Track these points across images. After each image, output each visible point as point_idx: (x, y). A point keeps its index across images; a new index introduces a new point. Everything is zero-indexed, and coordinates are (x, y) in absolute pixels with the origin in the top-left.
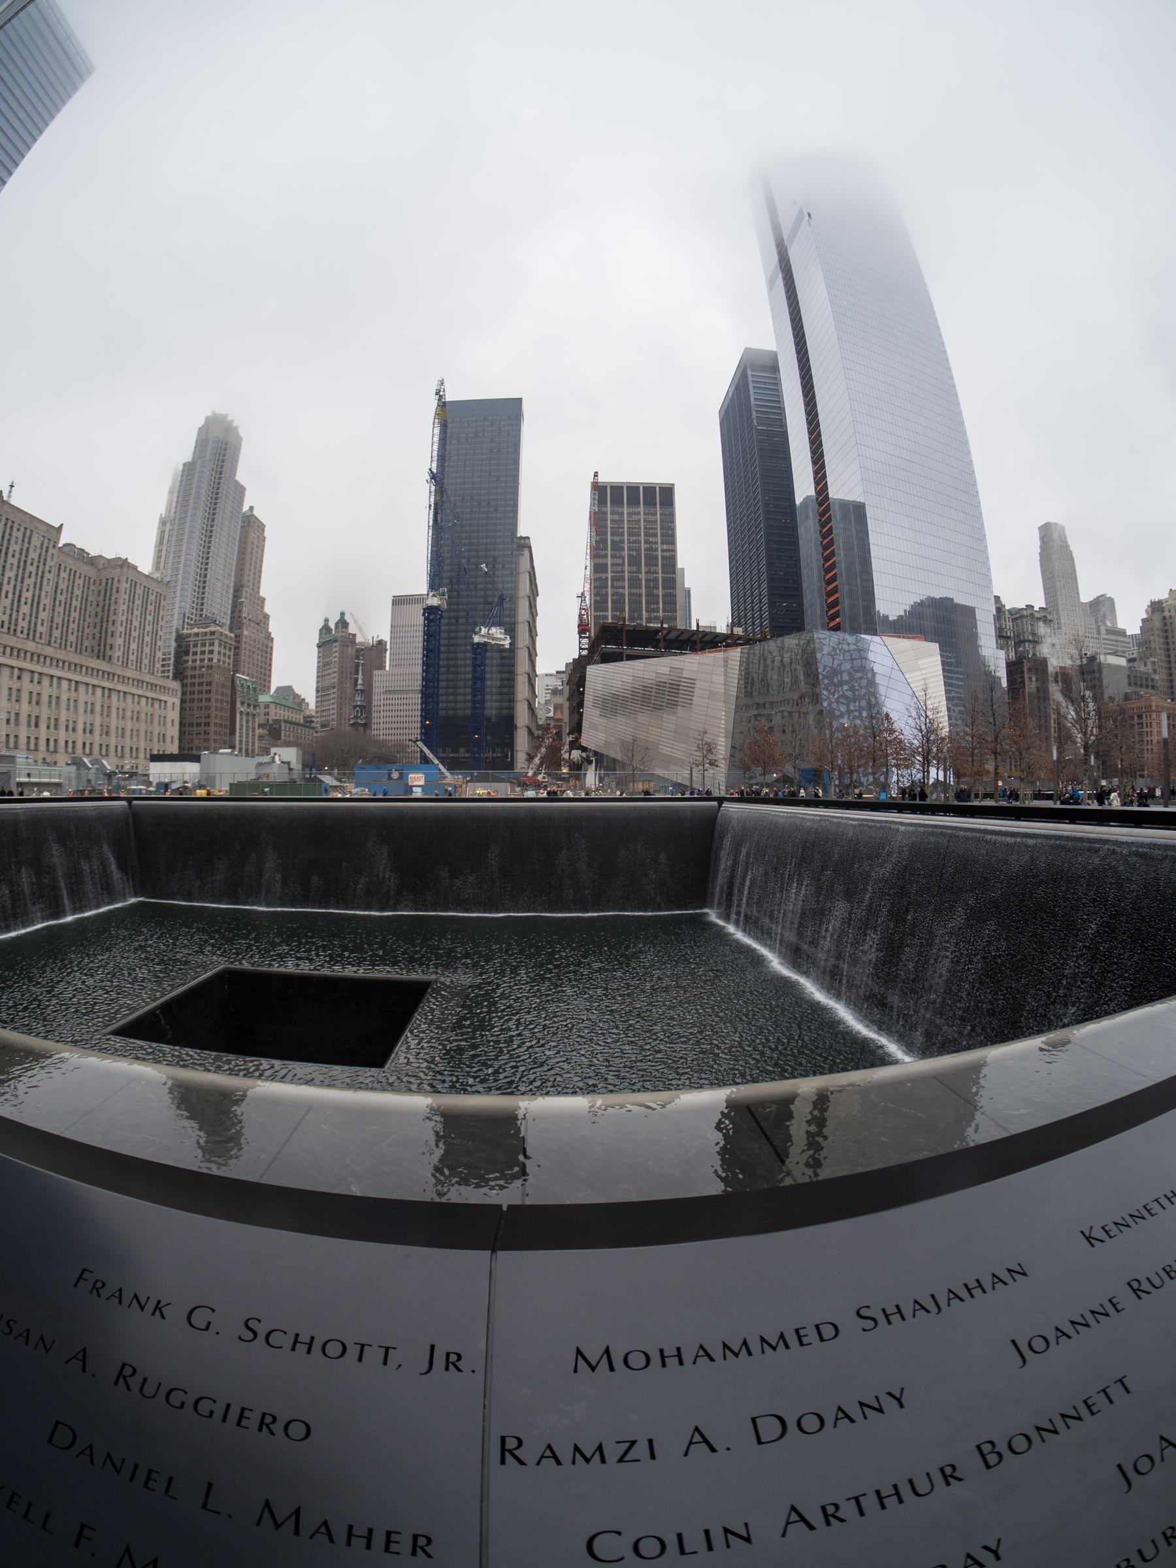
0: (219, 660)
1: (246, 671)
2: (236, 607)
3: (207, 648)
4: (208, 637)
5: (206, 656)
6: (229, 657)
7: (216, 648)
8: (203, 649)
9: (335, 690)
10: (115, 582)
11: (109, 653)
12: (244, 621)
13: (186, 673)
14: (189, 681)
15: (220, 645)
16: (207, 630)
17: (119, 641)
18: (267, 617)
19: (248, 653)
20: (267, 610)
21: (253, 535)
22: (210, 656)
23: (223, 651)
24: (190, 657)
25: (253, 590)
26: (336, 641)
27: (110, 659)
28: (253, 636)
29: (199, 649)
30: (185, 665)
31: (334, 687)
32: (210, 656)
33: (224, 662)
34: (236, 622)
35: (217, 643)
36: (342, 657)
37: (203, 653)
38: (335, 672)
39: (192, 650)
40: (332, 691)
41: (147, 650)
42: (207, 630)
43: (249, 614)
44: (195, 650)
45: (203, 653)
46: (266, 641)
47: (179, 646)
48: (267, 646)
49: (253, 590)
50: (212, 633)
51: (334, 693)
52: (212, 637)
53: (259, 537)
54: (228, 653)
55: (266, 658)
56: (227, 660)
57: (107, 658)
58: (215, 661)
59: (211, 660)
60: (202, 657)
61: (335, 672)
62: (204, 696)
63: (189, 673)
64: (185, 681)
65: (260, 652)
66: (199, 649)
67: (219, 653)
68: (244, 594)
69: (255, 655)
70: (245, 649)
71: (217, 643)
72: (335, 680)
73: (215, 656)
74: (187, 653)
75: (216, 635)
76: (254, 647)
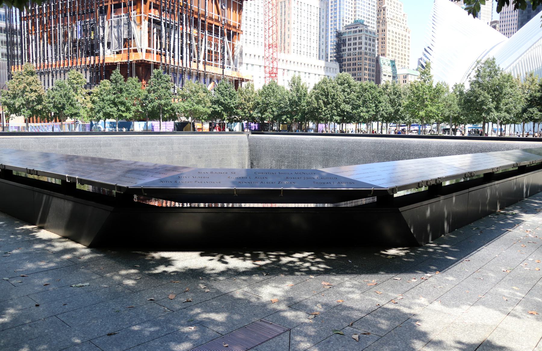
0: (366, 49)
3: (357, 41)
4: (358, 33)
5: (357, 46)
6: (374, 46)
7: (363, 40)
8: (355, 41)
10: (287, 3)
11: (287, 47)
12: (387, 20)
13: (344, 58)
14: (346, 62)
16: (357, 29)
17: (294, 39)
19: (391, 41)
22: (360, 46)
23: (368, 42)
24: (347, 47)
27: (288, 52)
29: (352, 42)
30: (343, 53)
32: (360, 46)
33: (370, 50)
35: (363, 38)
37: (355, 44)
39: (347, 42)
42: (357, 29)
44: (350, 42)
45: (355, 44)
47: (340, 40)
48: (405, 36)
50: (360, 31)
52: (360, 33)
54: (372, 43)
56: (372, 48)
57: (286, 51)
58: (363, 49)
59: (360, 48)
60: (355, 47)
62: (357, 72)
63: (346, 57)
64: (344, 63)
65: (400, 40)
66: (352, 42)
67: (366, 44)
69: (397, 43)
70: (389, 39)
71: (363, 38)
73: (363, 46)
74: (345, 45)
75: (364, 32)
76: (396, 37)
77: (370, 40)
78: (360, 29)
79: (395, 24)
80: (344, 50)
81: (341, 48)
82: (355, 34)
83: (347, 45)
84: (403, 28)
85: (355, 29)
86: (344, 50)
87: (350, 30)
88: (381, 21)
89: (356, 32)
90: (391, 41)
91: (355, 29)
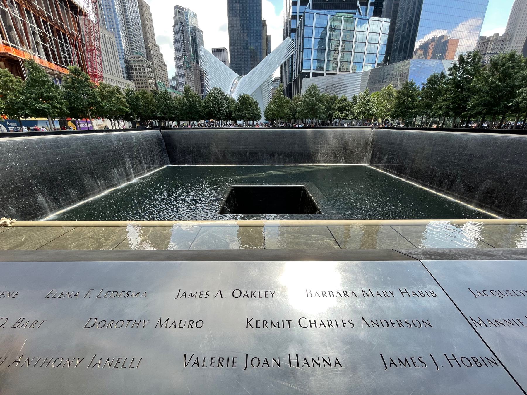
0: (148, 73)
1: (158, 79)
2: (147, 49)
4: (140, 62)
9: (194, 88)
15: (147, 67)
18: (161, 54)
20: (161, 51)
21: (145, 11)
24: (134, 71)
25: (152, 41)
26: (191, 67)
28: (158, 63)
31: (193, 86)
34: (149, 57)
36: (194, 74)
38: (193, 80)
39: (134, 68)
40: (193, 88)
41: (113, 66)
43: (154, 53)
46: (164, 66)
48: (164, 68)
49: (152, 41)
51: (194, 89)
53: (148, 14)
55: (165, 73)
59: (145, 73)
61: (193, 80)
67: (147, 70)
68: (149, 43)
72: (194, 83)
77: (149, 68)
78: (142, 59)
79: (157, 60)
80: (132, 73)
81: (130, 71)
82: (139, 62)
83: (134, 69)
84: (162, 63)
85: (138, 59)
86: (132, 73)
87: (134, 59)
88: (148, 56)
89: (139, 61)
90: (157, 70)
91: (138, 59)
